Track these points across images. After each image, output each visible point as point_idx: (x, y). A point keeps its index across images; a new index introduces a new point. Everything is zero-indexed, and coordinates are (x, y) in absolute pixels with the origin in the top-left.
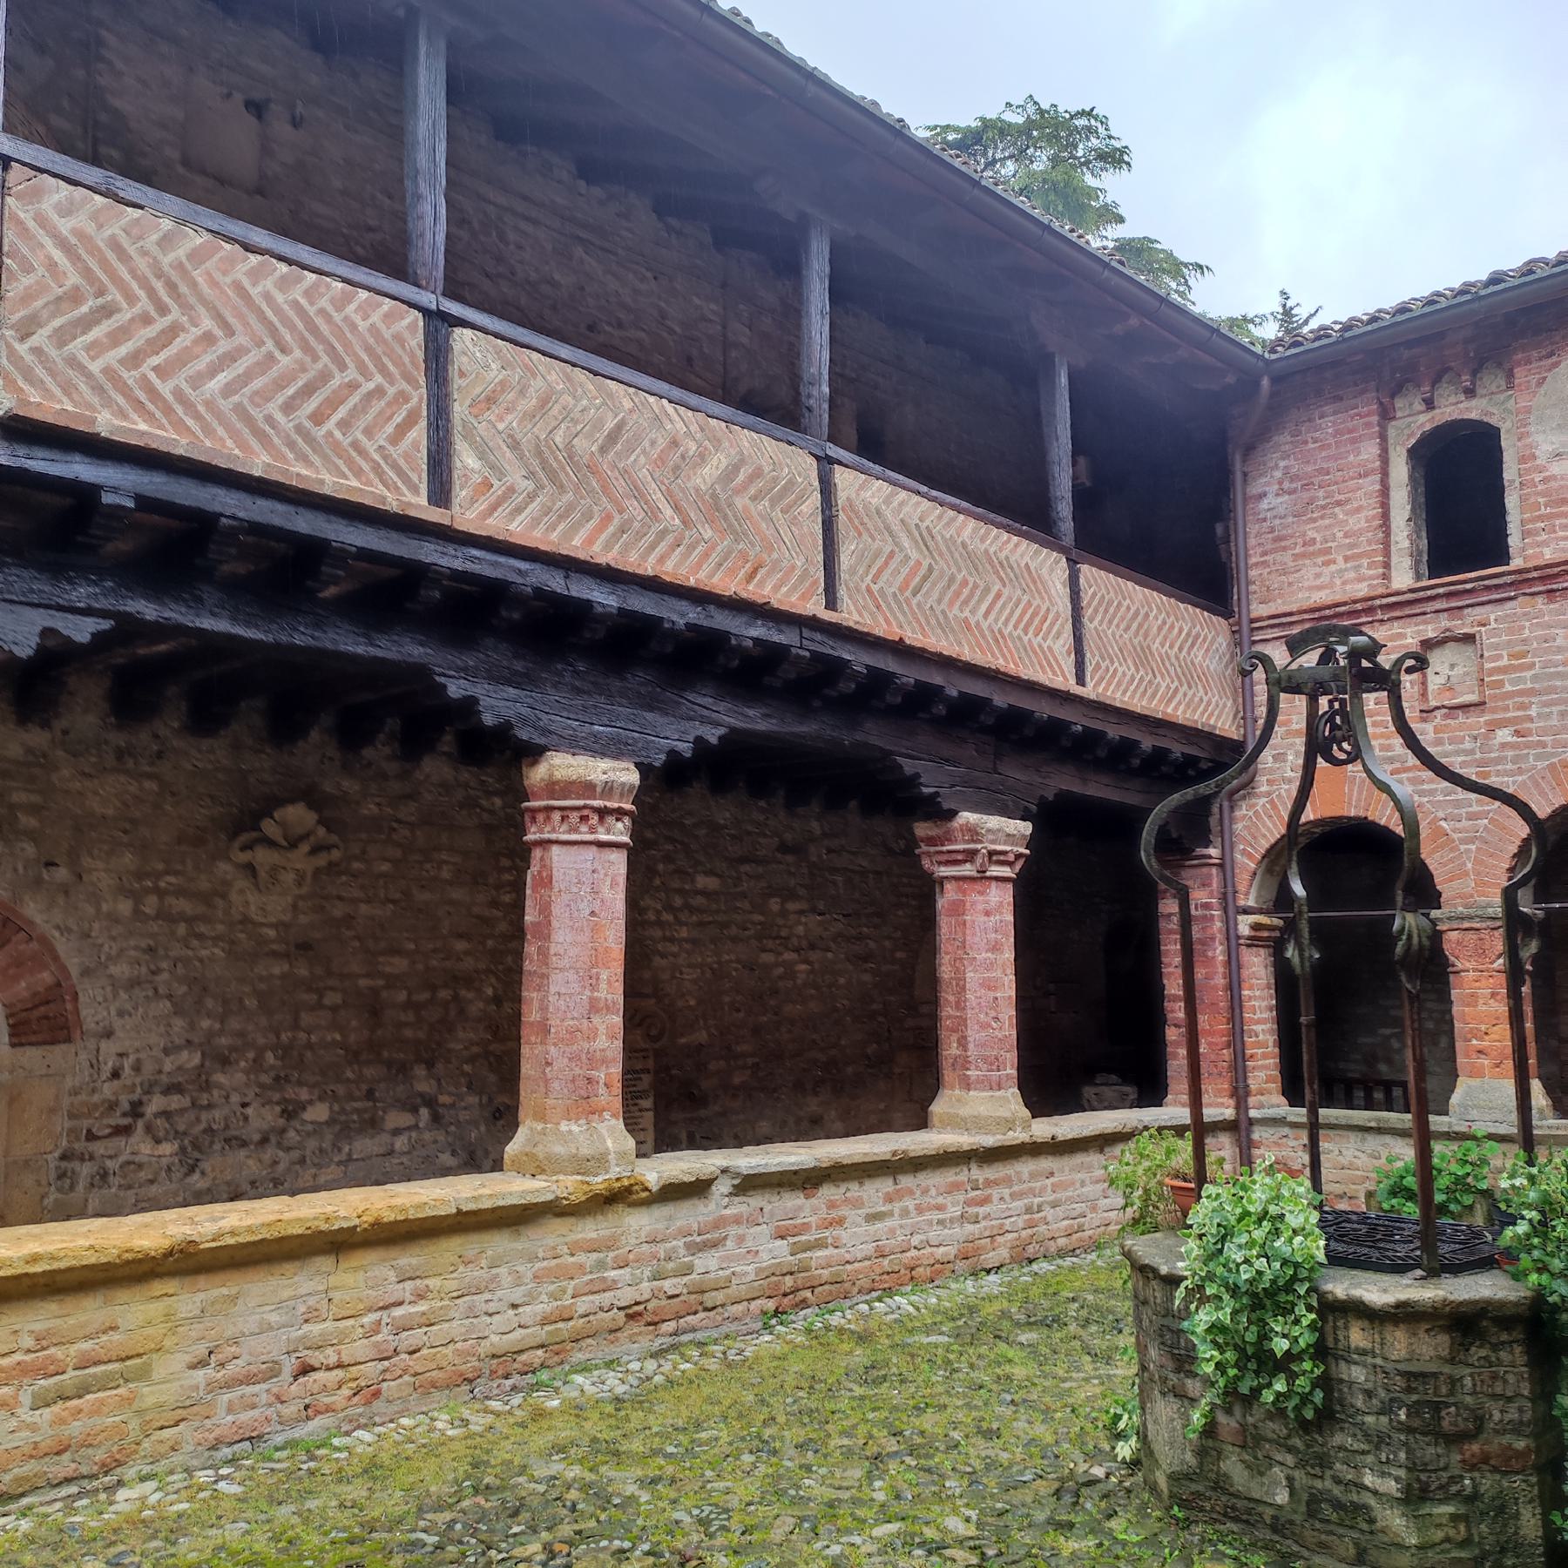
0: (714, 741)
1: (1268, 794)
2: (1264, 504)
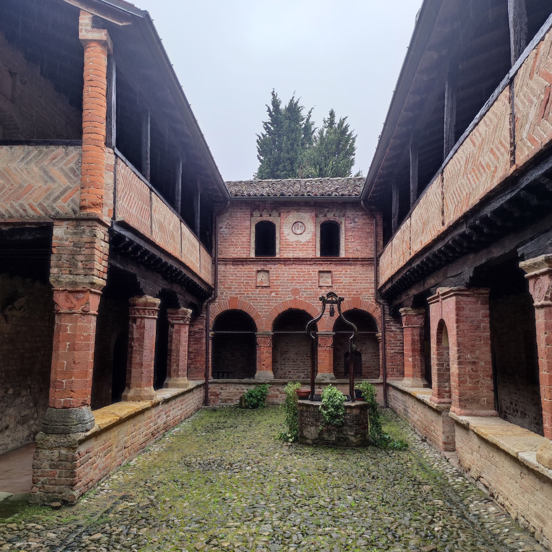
1: (219, 302)
2: (222, 230)
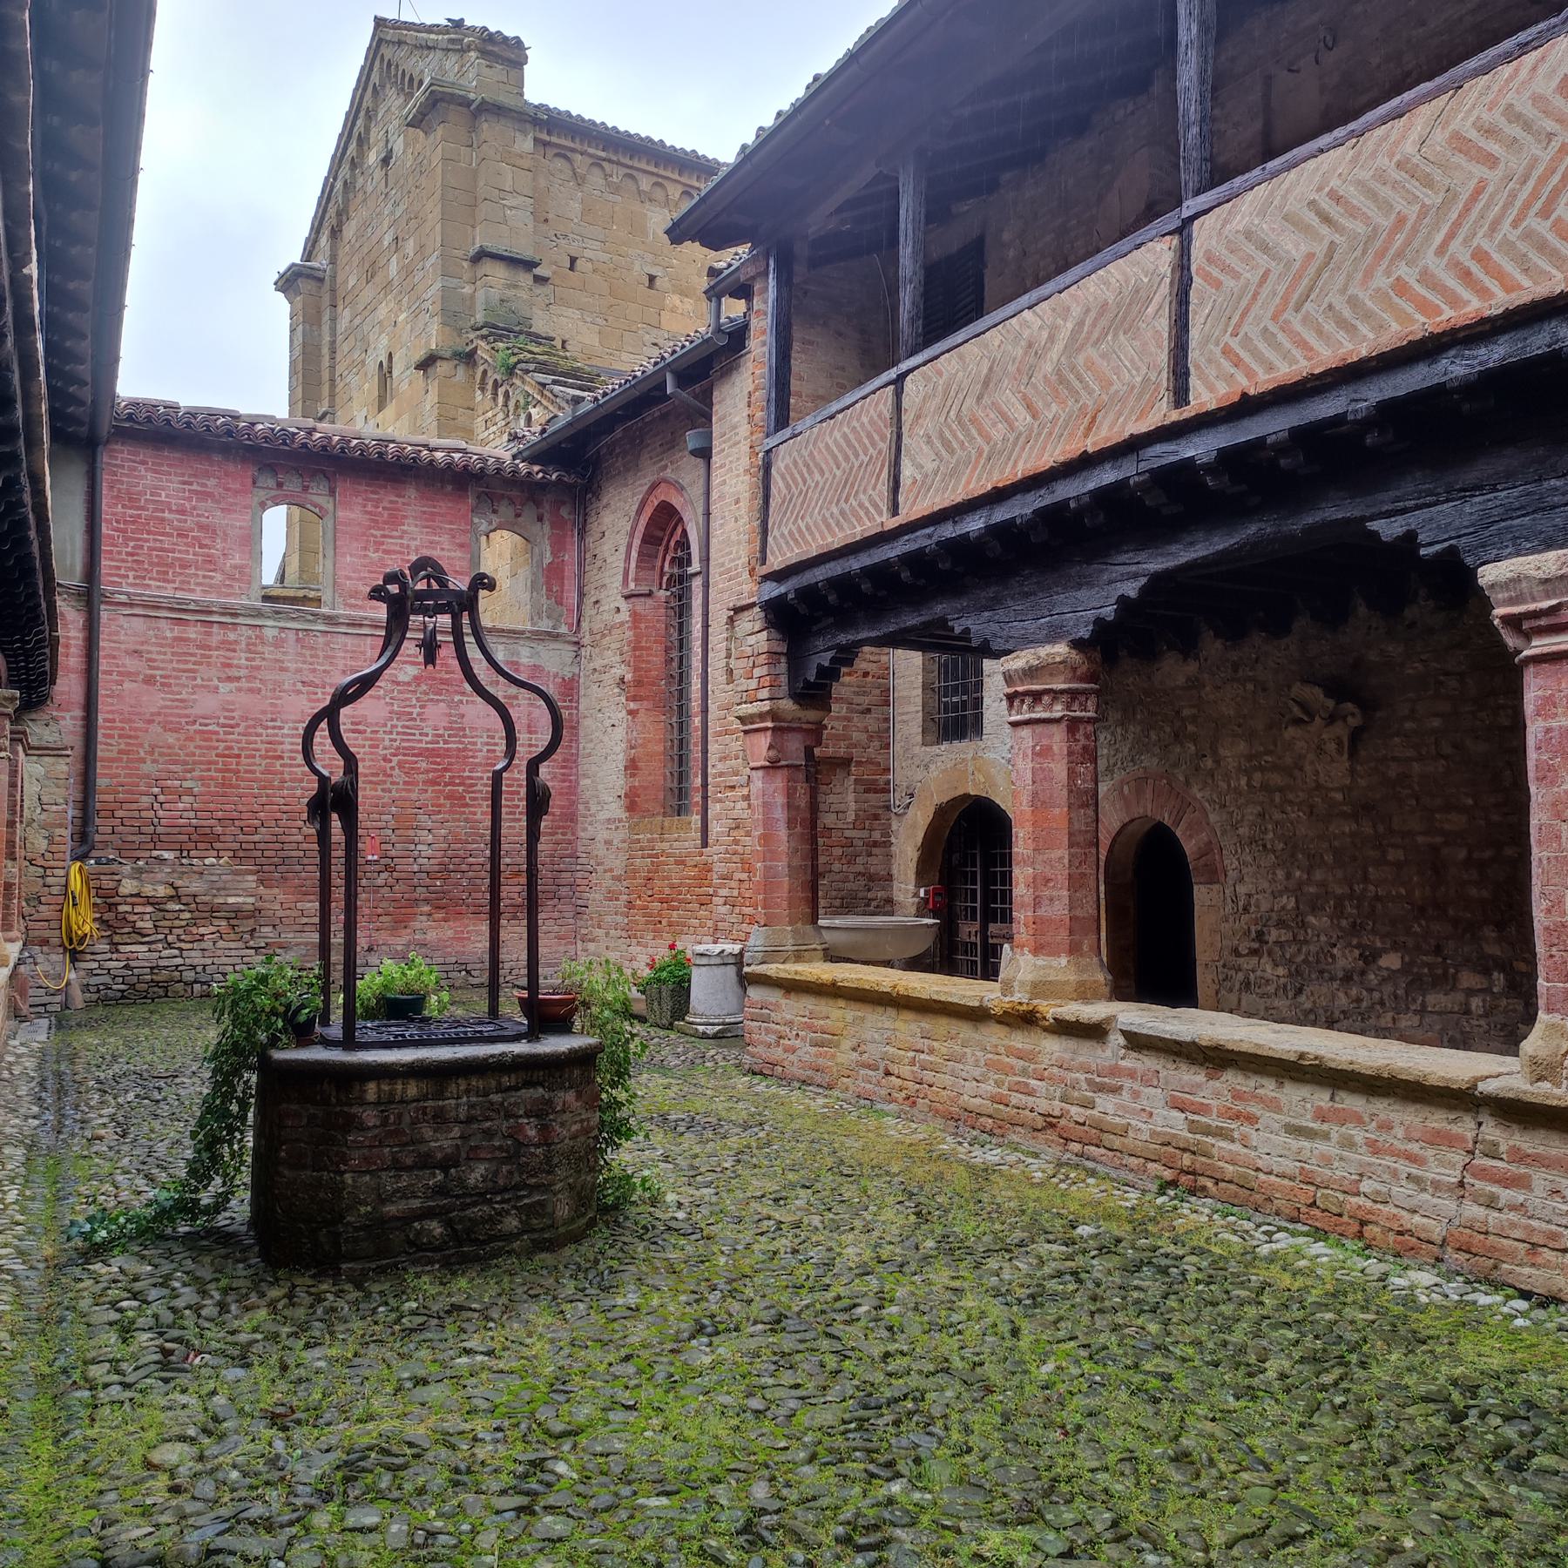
0: (1133, 594)
